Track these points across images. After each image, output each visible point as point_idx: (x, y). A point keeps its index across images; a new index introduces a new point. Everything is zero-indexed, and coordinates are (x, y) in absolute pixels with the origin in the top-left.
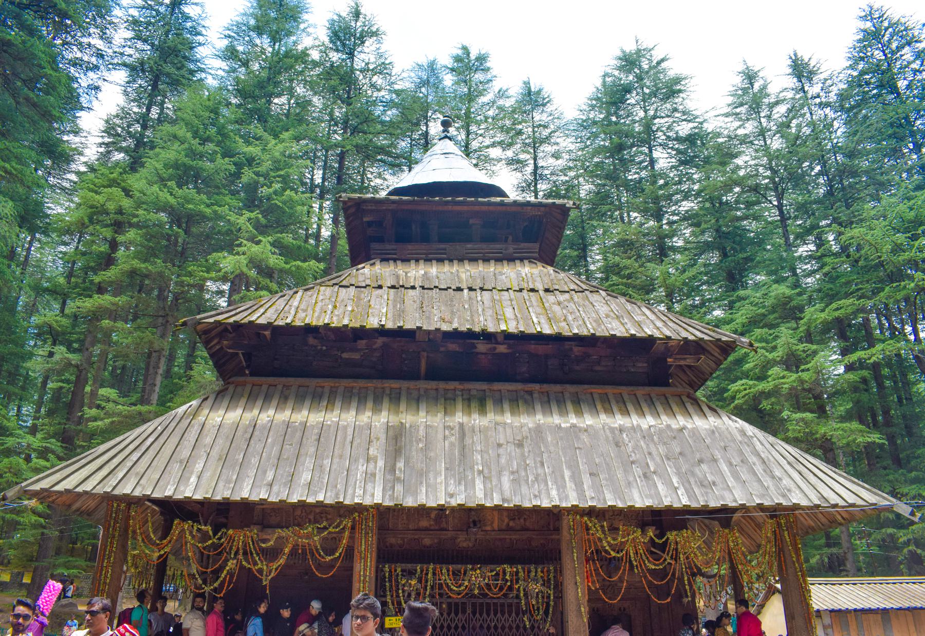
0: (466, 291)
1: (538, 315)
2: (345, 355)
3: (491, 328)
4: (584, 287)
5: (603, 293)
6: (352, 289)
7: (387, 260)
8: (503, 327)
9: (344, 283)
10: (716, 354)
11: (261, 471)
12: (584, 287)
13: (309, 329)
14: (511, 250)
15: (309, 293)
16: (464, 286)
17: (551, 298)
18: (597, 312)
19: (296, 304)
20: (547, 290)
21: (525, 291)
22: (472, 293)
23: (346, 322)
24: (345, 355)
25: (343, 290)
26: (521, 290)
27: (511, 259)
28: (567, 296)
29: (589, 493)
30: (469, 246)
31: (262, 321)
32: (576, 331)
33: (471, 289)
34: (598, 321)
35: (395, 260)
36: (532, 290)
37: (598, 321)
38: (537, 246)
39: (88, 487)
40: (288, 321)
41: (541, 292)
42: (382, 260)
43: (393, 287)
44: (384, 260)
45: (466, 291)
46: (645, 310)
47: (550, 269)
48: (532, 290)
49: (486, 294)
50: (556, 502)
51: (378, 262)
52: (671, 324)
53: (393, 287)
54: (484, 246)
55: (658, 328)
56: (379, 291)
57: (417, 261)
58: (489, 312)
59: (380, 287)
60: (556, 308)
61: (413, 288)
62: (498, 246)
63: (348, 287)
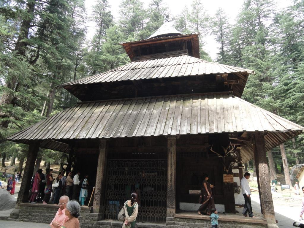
2: (113, 92)
10: (243, 79)
24: (113, 92)
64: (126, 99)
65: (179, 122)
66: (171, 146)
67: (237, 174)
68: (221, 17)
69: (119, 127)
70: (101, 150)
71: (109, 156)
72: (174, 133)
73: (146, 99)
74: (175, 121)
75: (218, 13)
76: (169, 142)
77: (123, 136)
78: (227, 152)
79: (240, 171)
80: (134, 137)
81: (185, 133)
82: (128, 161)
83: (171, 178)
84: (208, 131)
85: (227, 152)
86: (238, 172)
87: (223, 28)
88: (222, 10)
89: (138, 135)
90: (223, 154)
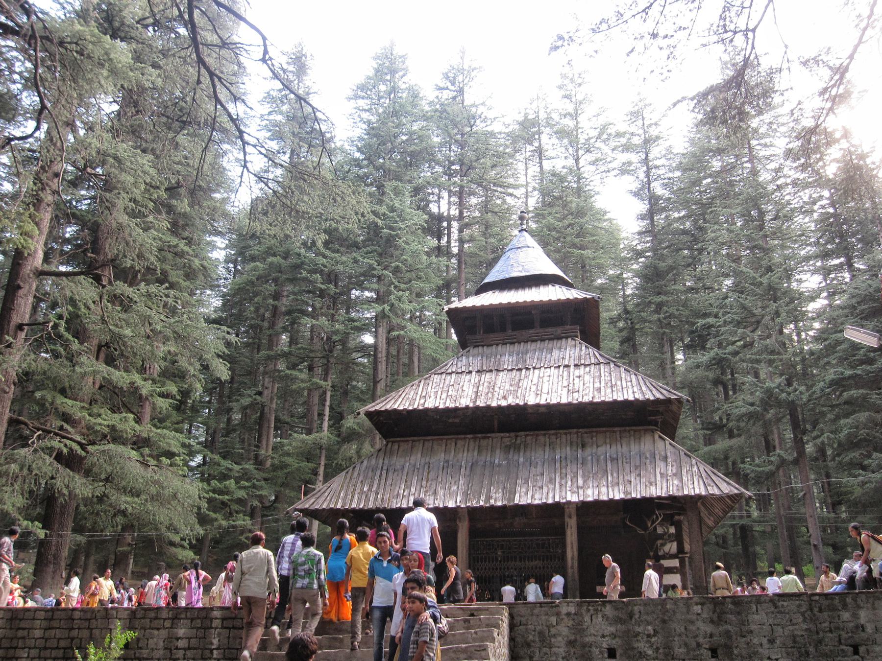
0: (524, 371)
4: (601, 360)
5: (612, 365)
6: (454, 375)
7: (478, 346)
9: (450, 371)
14: (559, 332)
17: (577, 373)
19: (420, 392)
20: (576, 365)
21: (561, 368)
22: (528, 372)
24: (450, 421)
25: (448, 377)
26: (559, 367)
28: (588, 369)
30: (531, 331)
31: (401, 408)
33: (527, 369)
40: (415, 406)
41: (572, 367)
42: (475, 347)
43: (478, 372)
45: (524, 371)
46: (633, 377)
48: (567, 366)
52: (644, 388)
53: (478, 372)
54: (541, 330)
55: (634, 392)
56: (468, 377)
57: (497, 345)
58: (534, 388)
61: (491, 371)
62: (550, 330)
64: (480, 435)
65: (580, 482)
66: (570, 517)
67: (676, 568)
68: (647, 123)
69: (489, 491)
70: (460, 525)
71: (473, 534)
72: (574, 498)
73: (517, 436)
74: (574, 480)
75: (636, 109)
76: (567, 510)
77: (499, 504)
78: (652, 524)
79: (680, 563)
80: (517, 505)
81: (590, 499)
82: (503, 541)
83: (573, 563)
84: (622, 496)
85: (652, 524)
86: (678, 565)
87: (651, 156)
88: (647, 102)
89: (523, 502)
90: (646, 528)
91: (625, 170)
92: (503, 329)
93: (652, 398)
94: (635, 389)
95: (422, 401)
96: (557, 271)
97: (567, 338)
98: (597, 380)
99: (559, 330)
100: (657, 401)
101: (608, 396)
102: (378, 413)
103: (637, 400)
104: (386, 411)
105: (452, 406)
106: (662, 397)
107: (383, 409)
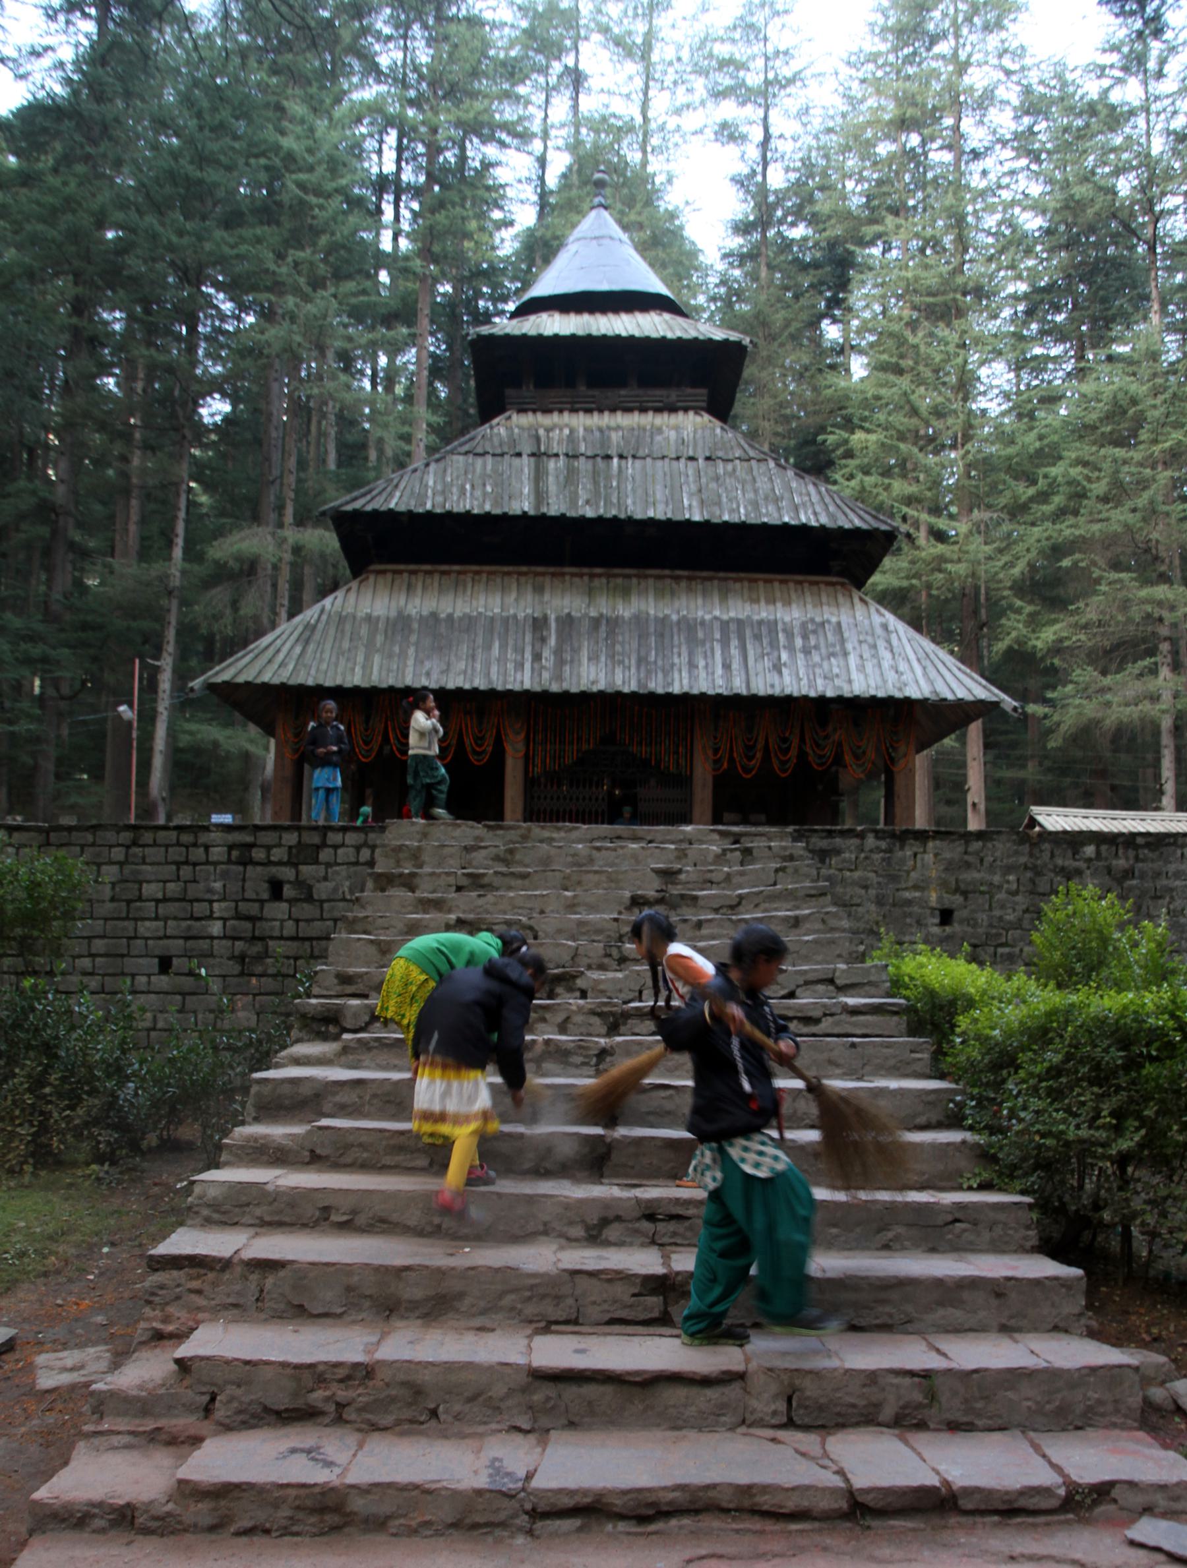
1: (691, 495)
3: (639, 516)
4: (752, 453)
5: (772, 464)
6: (489, 459)
8: (651, 514)
9: (479, 450)
11: (419, 662)
12: (752, 453)
13: (449, 515)
15: (442, 464)
16: (613, 451)
18: (756, 491)
20: (708, 459)
23: (487, 508)
25: (479, 461)
27: (673, 409)
28: (730, 467)
29: (719, 682)
30: (623, 392)
31: (402, 508)
32: (726, 518)
33: (621, 457)
34: (755, 505)
35: (534, 411)
36: (692, 459)
37: (755, 505)
38: (704, 391)
39: (266, 678)
40: (429, 506)
42: (520, 411)
43: (533, 455)
44: (521, 411)
46: (811, 488)
47: (718, 423)
48: (692, 459)
49: (638, 463)
50: (686, 689)
51: (515, 417)
52: (832, 508)
53: (533, 455)
54: (641, 392)
59: (519, 455)
60: (713, 485)
62: (658, 392)
63: (485, 453)
91: (728, 133)
92: (571, 384)
93: (847, 526)
94: (818, 509)
95: (439, 499)
96: (663, 290)
97: (686, 410)
98: (748, 487)
99: (673, 395)
100: (857, 531)
101: (770, 515)
102: (357, 514)
103: (823, 527)
104: (375, 512)
105: (497, 511)
106: (864, 526)
107: (369, 508)
